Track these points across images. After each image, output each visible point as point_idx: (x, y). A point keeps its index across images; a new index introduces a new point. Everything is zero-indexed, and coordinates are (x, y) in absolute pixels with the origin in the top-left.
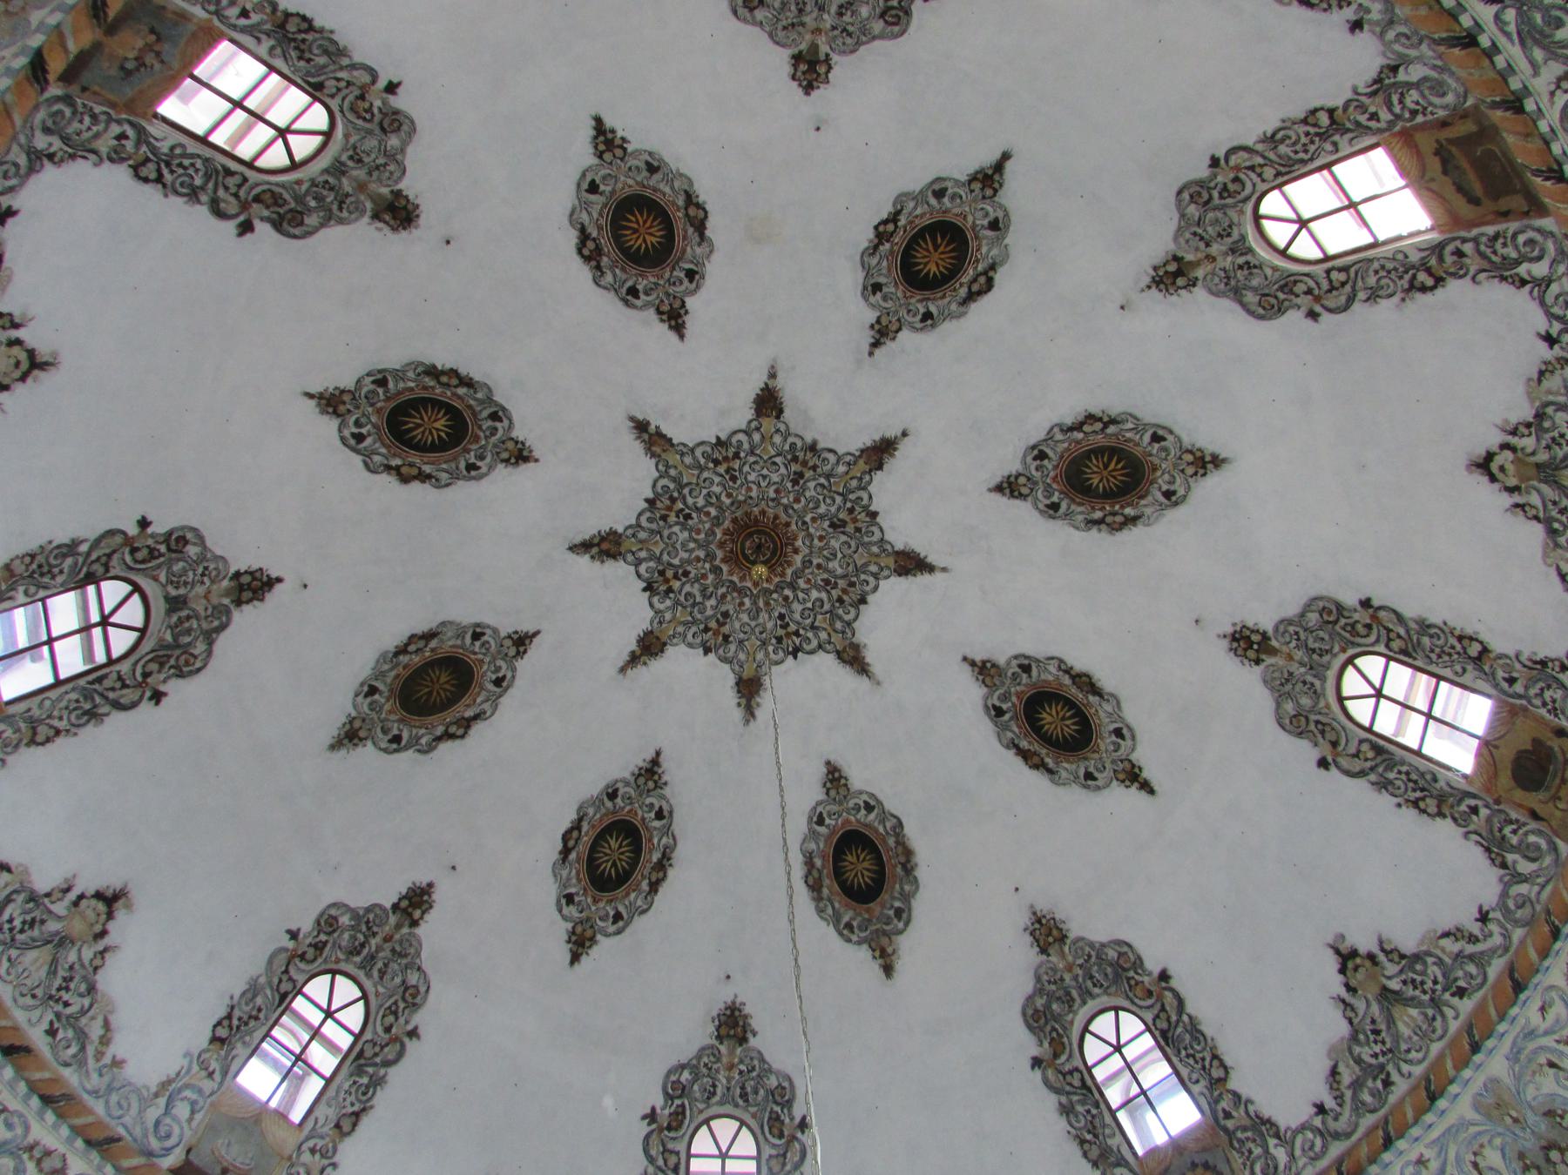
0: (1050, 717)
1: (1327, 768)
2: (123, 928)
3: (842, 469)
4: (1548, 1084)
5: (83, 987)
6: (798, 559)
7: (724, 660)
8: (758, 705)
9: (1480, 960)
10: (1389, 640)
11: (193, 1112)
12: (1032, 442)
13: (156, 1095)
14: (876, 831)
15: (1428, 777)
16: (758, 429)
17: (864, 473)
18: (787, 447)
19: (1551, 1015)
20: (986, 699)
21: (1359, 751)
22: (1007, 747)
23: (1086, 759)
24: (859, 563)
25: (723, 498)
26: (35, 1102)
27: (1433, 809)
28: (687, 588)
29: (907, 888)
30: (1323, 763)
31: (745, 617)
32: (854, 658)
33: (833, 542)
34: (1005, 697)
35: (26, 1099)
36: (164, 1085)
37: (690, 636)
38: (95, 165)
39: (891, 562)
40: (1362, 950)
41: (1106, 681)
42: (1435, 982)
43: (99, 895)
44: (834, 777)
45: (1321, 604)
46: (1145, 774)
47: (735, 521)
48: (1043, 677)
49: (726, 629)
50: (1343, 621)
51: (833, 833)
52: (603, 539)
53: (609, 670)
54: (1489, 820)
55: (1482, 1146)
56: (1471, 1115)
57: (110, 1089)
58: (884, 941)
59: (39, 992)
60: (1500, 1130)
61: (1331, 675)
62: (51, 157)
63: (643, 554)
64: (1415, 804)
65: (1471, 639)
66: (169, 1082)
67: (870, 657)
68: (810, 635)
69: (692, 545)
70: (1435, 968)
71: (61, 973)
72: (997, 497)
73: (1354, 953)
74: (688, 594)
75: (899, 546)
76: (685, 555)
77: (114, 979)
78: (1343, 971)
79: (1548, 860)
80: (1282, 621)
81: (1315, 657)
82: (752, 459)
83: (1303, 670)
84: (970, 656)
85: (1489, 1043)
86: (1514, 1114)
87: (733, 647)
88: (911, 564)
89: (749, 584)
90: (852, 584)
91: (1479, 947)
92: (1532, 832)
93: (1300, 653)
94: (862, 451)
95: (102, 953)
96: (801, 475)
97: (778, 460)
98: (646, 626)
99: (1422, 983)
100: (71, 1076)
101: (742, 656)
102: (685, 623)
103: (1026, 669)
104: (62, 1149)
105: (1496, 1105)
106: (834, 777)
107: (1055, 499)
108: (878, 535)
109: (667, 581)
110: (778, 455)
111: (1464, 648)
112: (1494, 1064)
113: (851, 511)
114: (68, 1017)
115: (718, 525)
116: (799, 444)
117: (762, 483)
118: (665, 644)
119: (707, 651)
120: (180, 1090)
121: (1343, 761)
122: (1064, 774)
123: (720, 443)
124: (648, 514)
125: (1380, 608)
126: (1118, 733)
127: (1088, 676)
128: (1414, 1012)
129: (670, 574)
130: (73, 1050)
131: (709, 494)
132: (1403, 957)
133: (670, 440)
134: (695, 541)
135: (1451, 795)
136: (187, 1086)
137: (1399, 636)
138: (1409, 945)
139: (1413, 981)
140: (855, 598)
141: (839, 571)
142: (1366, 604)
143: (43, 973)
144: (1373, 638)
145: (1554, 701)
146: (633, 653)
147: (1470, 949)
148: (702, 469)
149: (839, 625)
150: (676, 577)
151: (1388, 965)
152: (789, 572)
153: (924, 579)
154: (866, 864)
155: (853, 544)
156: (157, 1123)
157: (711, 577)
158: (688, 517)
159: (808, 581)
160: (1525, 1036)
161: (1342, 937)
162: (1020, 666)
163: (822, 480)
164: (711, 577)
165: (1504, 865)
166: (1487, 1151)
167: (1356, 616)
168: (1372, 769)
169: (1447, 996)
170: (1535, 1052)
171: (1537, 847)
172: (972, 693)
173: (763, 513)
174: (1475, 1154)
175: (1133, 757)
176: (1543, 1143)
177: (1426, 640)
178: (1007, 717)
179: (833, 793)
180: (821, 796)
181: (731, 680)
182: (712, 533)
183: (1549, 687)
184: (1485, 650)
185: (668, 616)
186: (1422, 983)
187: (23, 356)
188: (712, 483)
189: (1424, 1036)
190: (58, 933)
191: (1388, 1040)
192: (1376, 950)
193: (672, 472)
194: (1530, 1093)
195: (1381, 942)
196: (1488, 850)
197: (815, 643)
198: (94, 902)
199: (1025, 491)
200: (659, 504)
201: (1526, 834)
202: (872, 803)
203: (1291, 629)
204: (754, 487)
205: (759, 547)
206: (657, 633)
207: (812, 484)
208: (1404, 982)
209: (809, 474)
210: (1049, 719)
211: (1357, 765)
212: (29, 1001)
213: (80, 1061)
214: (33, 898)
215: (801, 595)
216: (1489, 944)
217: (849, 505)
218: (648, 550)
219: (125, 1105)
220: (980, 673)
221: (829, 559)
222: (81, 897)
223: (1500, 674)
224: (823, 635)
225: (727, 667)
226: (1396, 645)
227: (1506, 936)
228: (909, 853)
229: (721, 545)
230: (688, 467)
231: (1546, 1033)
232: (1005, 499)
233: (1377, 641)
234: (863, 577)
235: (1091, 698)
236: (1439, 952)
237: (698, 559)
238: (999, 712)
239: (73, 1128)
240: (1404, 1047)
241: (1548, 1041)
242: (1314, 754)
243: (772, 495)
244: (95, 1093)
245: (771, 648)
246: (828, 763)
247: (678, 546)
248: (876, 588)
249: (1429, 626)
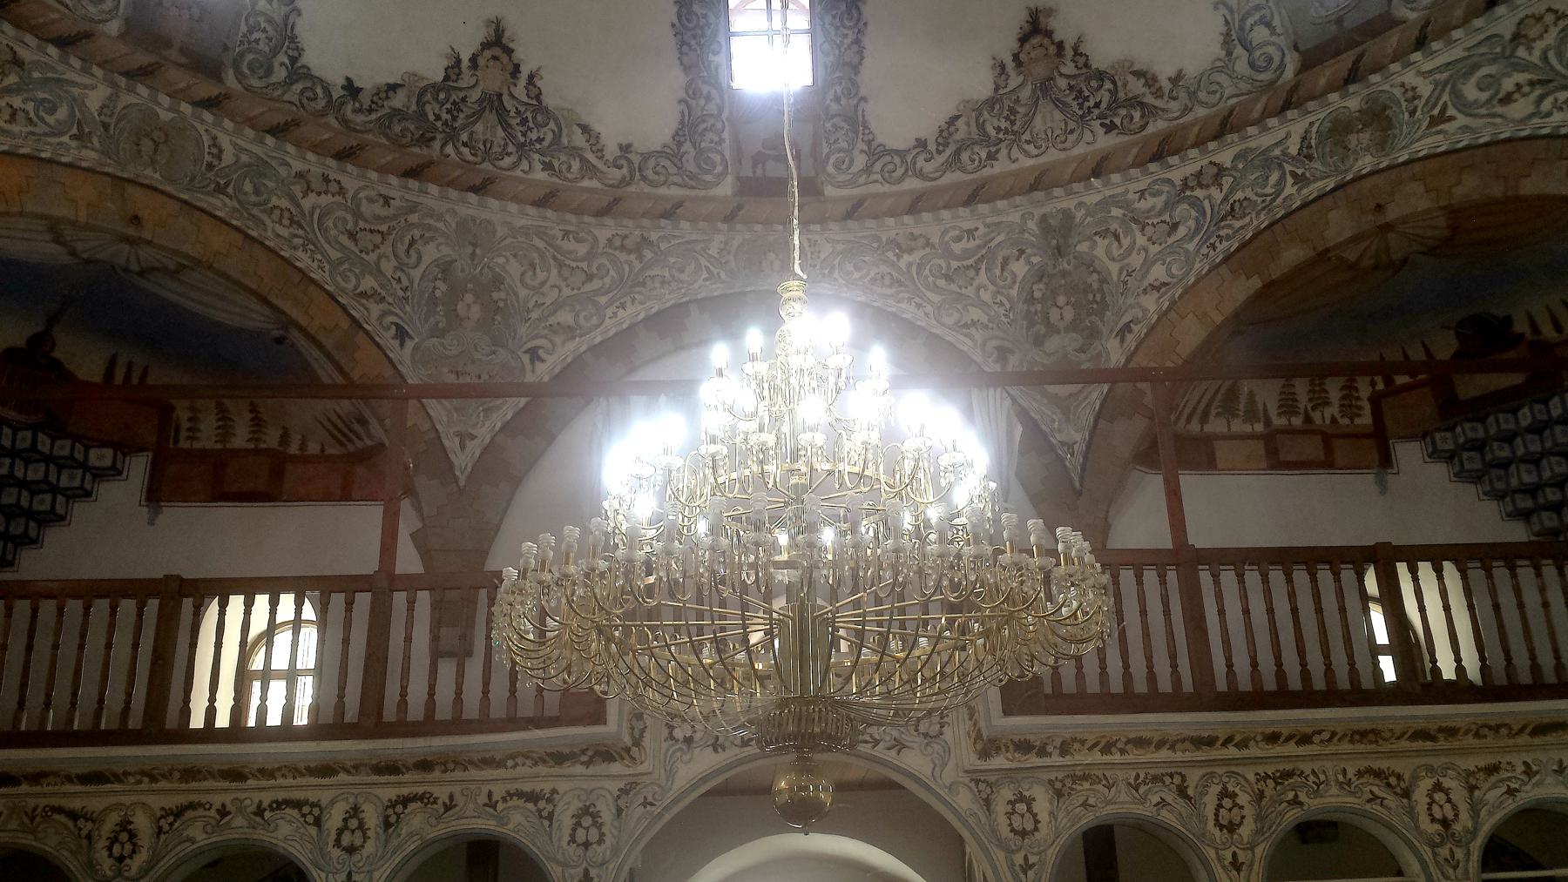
2: (1063, 30)
5: (1094, 83)
11: (1268, 25)
13: (1229, 54)
26: (1153, 167)
35: (1146, 173)
36: (1227, 43)
38: (300, 15)
43: (1023, 40)
57: (1193, 95)
59: (1072, 125)
62: (294, 60)
66: (1228, 34)
71: (1069, 100)
77: (1105, 51)
95: (1077, 52)
100: (1157, 126)
104: (1206, 162)
114: (1108, 108)
120: (1242, 29)
130: (1137, 115)
136: (1243, 20)
143: (1058, 116)
156: (1252, 65)
187: (488, 54)
190: (1034, 91)
198: (1027, 47)
212: (1071, 138)
213: (1149, 112)
214: (991, 103)
219: (1215, 87)
222: (1016, 57)
239: (1195, 145)
244: (1186, 110)
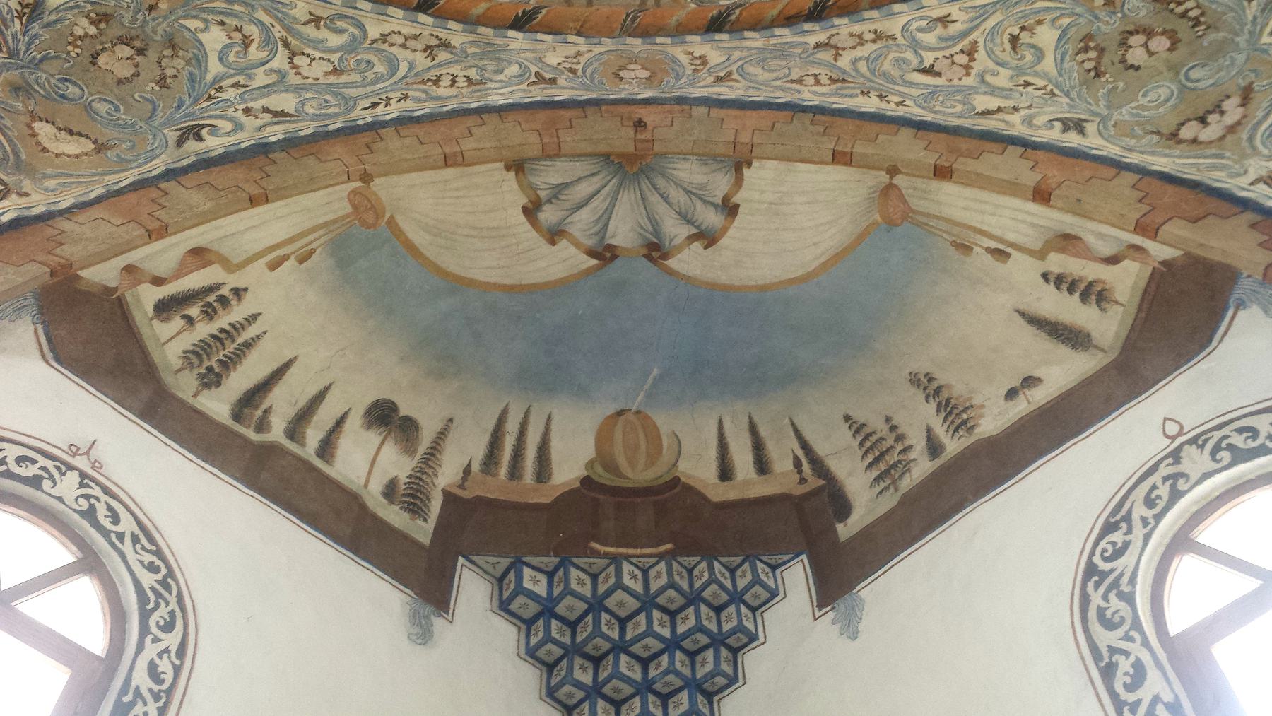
55: (1040, 22)
60: (1079, 10)
174: (1023, 28)
176: (1131, 28)
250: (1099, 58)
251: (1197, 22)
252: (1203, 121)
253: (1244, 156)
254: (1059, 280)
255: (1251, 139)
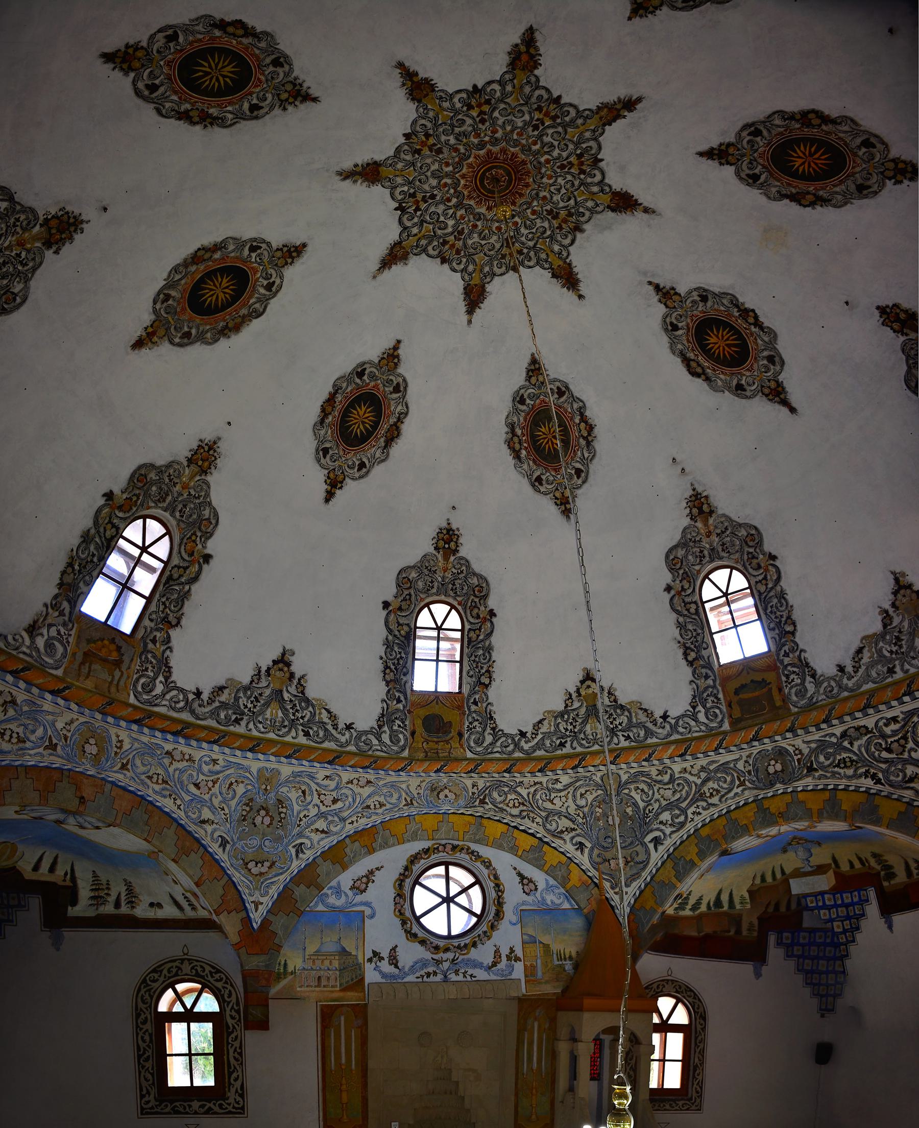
0: (363, 413)
1: (384, 608)
3: (556, 248)
4: (294, 795)
6: (483, 210)
7: (398, 150)
8: (355, 182)
9: (328, 736)
10: (474, 630)
12: (571, 387)
14: (251, 297)
15: (405, 670)
16: (602, 191)
17: (551, 264)
18: (581, 210)
19: (326, 782)
20: (370, 362)
21: (402, 625)
22: (334, 385)
23: (338, 446)
24: (475, 257)
25: (546, 157)
27: (388, 678)
28: (469, 121)
29: (209, 335)
30: (386, 605)
31: (435, 167)
32: (395, 256)
33: (495, 238)
34: (372, 376)
37: (423, 122)
39: (476, 281)
40: (293, 668)
41: (397, 449)
42: (302, 718)
44: (292, 253)
45: (484, 585)
46: (338, 492)
47: (524, 163)
48: (392, 402)
49: (426, 151)
50: (477, 600)
51: (245, 262)
52: (532, 57)
53: (403, 54)
54: (398, 710)
56: (254, 771)
58: (161, 332)
61: (443, 598)
63: (509, 88)
64: (387, 667)
65: (490, 677)
67: (397, 269)
68: (416, 220)
69: (509, 128)
70: (309, 714)
72: (528, 359)
73: (288, 665)
74: (463, 122)
75: (489, 288)
76: (500, 122)
78: (275, 662)
79: (395, 748)
80: (467, 561)
81: (451, 586)
82: (577, 183)
83: (440, 579)
84: (402, 345)
85: (294, 761)
86: (268, 788)
87: (409, 157)
88: (474, 297)
89: (464, 171)
90: (458, 252)
91: (334, 732)
92: (405, 735)
93: (446, 571)
94: (570, 264)
96: (556, 217)
97: (572, 202)
98: (440, 85)
99: (297, 711)
101: (400, 166)
102: (436, 118)
103: (397, 389)
105: (267, 779)
106: (292, 253)
107: (528, 401)
108: (498, 271)
109: (479, 105)
110: (576, 202)
111: (483, 674)
112: (286, 769)
113: (520, 252)
115: (522, 151)
116: (582, 219)
117: (556, 189)
118: (419, 101)
119: (407, 136)
121: (392, 616)
122: (322, 432)
123: (597, 161)
124: (546, 96)
125: (492, 623)
126: (362, 465)
127: (398, 435)
128: (280, 714)
129: (486, 108)
131: (552, 146)
132: (303, 693)
133: (610, 125)
134: (512, 131)
135: (401, 686)
137: (478, 636)
138: (311, 693)
139: (295, 705)
140: (447, 255)
141: (470, 242)
142: (492, 614)
144: (472, 620)
145: (474, 728)
146: (417, 74)
147: (330, 727)
148: (577, 144)
149: (423, 242)
150: (482, 113)
151: (294, 687)
152: (472, 203)
153: (462, 307)
154: (221, 295)
155: (492, 253)
157: (476, 141)
158: (536, 127)
159: (462, 217)
160: (309, 775)
161: (293, 654)
162: (398, 384)
163: (548, 233)
164: (476, 141)
165: (380, 727)
166: (241, 785)
167: (482, 608)
168: (395, 636)
169: (300, 728)
170: (305, 783)
171: (399, 741)
172: (372, 351)
173: (527, 185)
175: (347, 479)
176: (264, 806)
177: (481, 652)
178: (358, 381)
179: (279, 254)
180: (274, 245)
181: (379, 157)
182: (516, 144)
183: (480, 723)
184: (487, 686)
185: (446, 105)
186: (297, 711)
188: (562, 150)
189: (273, 726)
191: (258, 708)
192: (297, 676)
193: (580, 121)
194: (285, 789)
195: (303, 677)
196: (383, 715)
197: (408, 224)
199: (533, 380)
200: (552, 107)
201: (402, 732)
202: (274, 289)
203: (464, 568)
204: (551, 181)
205: (498, 181)
206: (431, 95)
207: (546, 224)
208: (291, 701)
209: (555, 223)
210: (361, 413)
211: (393, 626)
215: (451, 212)
216: (338, 736)
217: (525, 251)
218: (512, 93)
220: (389, 355)
221: (480, 235)
223: (477, 697)
224: (415, 230)
225: (392, 153)
226: (472, 634)
227: (348, 743)
228: (237, 328)
229: (503, 151)
230: (582, 133)
231: (317, 784)
232: (526, 365)
233: (471, 623)
234: (464, 260)
235: (382, 440)
236: (317, 712)
237: (495, 132)
238: (360, 374)
240: (260, 719)
241: (314, 787)
242: (389, 598)
243: (542, 194)
245: (406, 188)
246: (304, 245)
247: (509, 118)
248: (454, 270)
249: (489, 653)
250: (249, 812)
251: (280, 821)
252: (257, 864)
253: (257, 888)
254: (186, 897)
255: (262, 883)
